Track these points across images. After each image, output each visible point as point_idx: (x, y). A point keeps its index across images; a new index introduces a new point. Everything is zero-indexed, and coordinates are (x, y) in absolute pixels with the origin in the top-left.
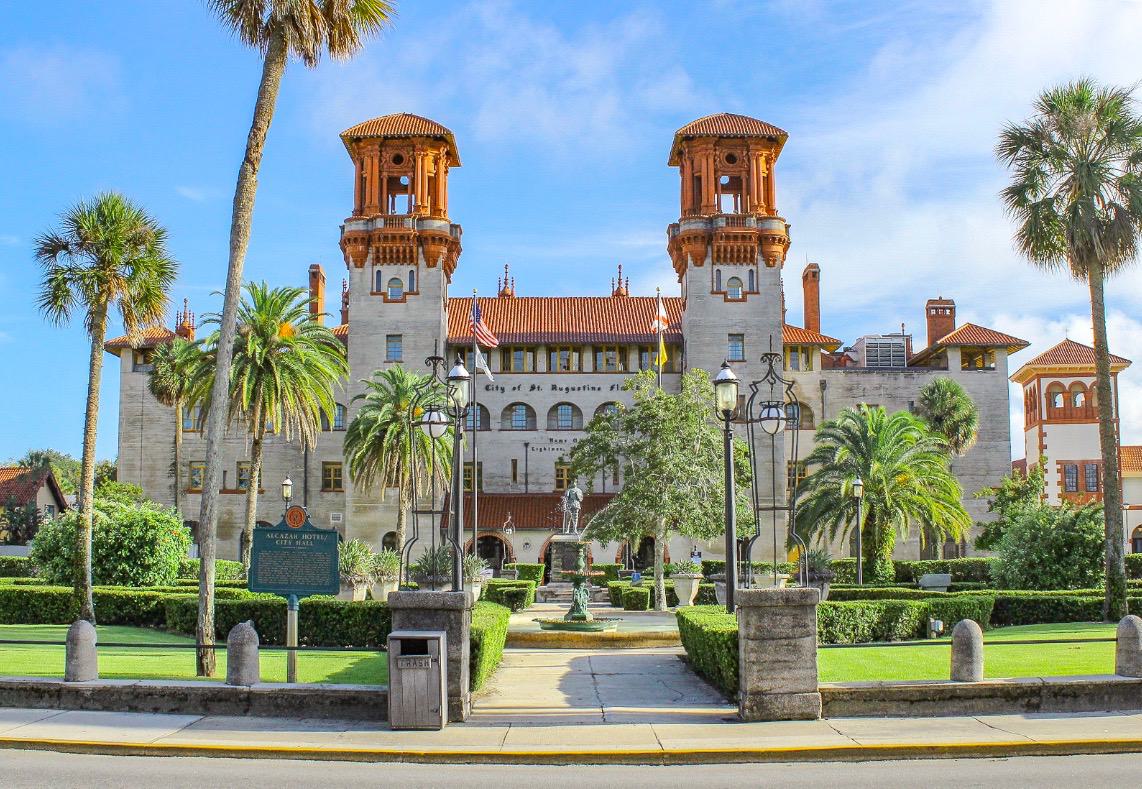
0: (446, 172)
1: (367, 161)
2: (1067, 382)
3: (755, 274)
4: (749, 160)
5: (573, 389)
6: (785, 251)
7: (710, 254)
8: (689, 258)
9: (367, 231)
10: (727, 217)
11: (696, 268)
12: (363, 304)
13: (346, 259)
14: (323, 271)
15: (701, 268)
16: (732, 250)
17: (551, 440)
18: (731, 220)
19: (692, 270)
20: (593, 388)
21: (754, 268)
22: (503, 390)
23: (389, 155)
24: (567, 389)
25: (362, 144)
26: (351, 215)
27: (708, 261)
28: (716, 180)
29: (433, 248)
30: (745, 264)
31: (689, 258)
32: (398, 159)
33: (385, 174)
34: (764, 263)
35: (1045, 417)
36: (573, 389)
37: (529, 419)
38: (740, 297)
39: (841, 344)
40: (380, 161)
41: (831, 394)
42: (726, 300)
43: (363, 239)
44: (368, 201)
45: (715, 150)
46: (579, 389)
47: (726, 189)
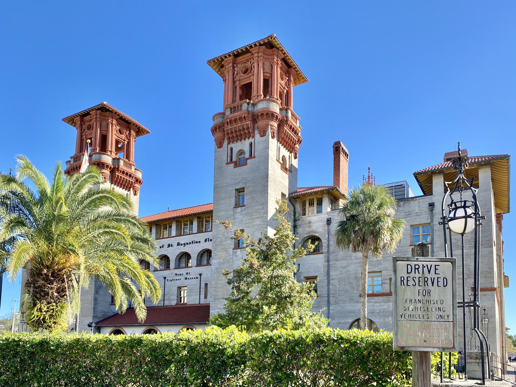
3: (253, 144)
11: (219, 149)
15: (221, 149)
17: (176, 274)
34: (259, 135)
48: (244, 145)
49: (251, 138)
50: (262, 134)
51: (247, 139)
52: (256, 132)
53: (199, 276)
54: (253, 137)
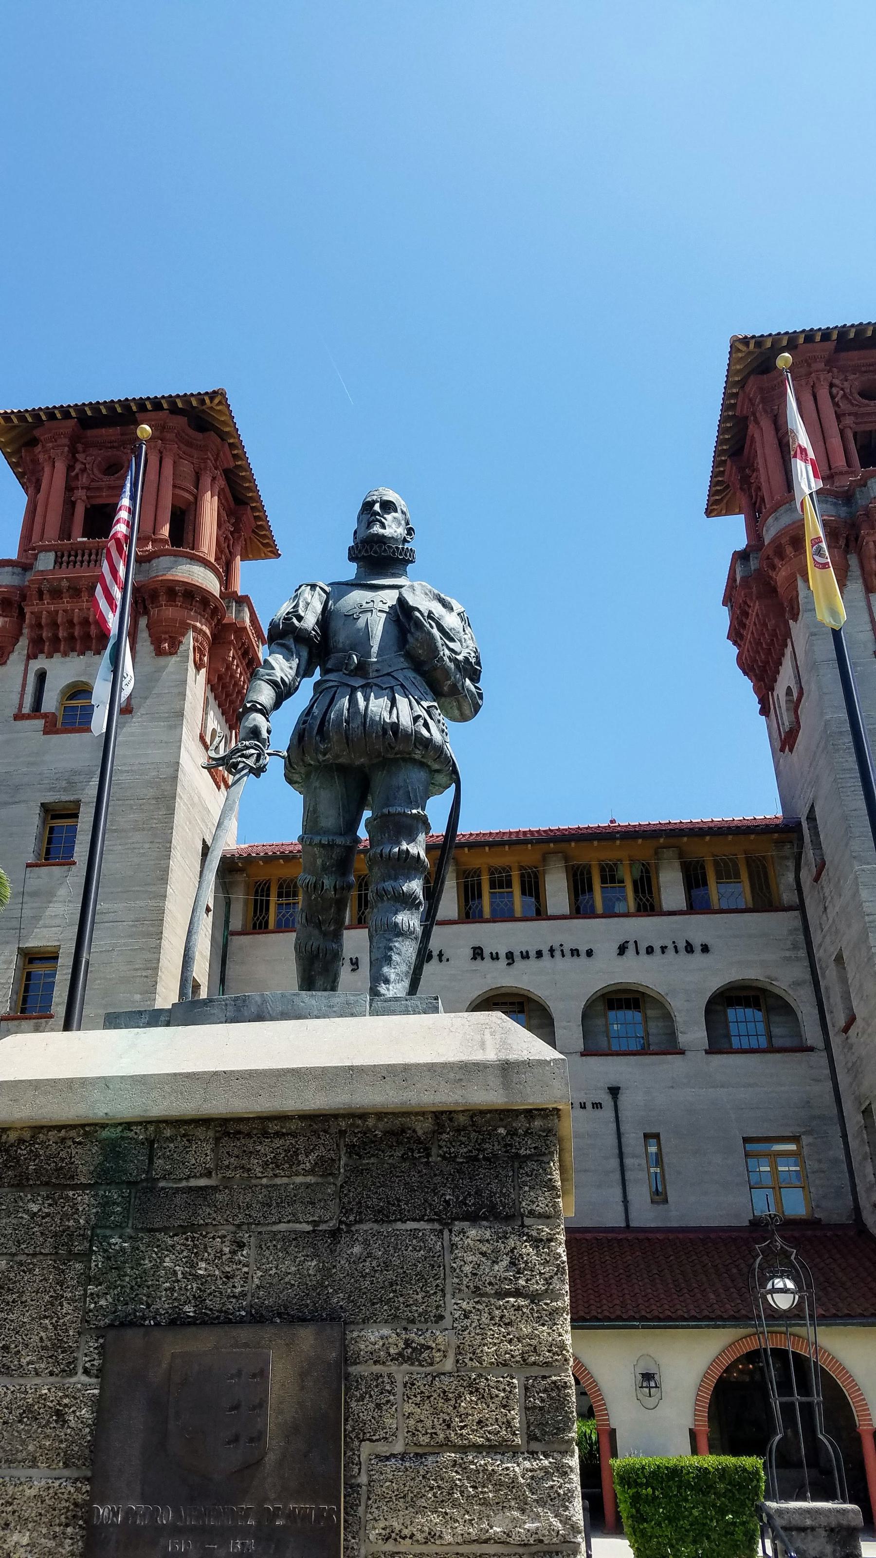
5: (525, 956)
20: (575, 952)
24: (510, 956)
29: (170, 612)
33: (81, 494)
36: (525, 956)
40: (70, 468)
46: (539, 954)
53: (606, 1099)
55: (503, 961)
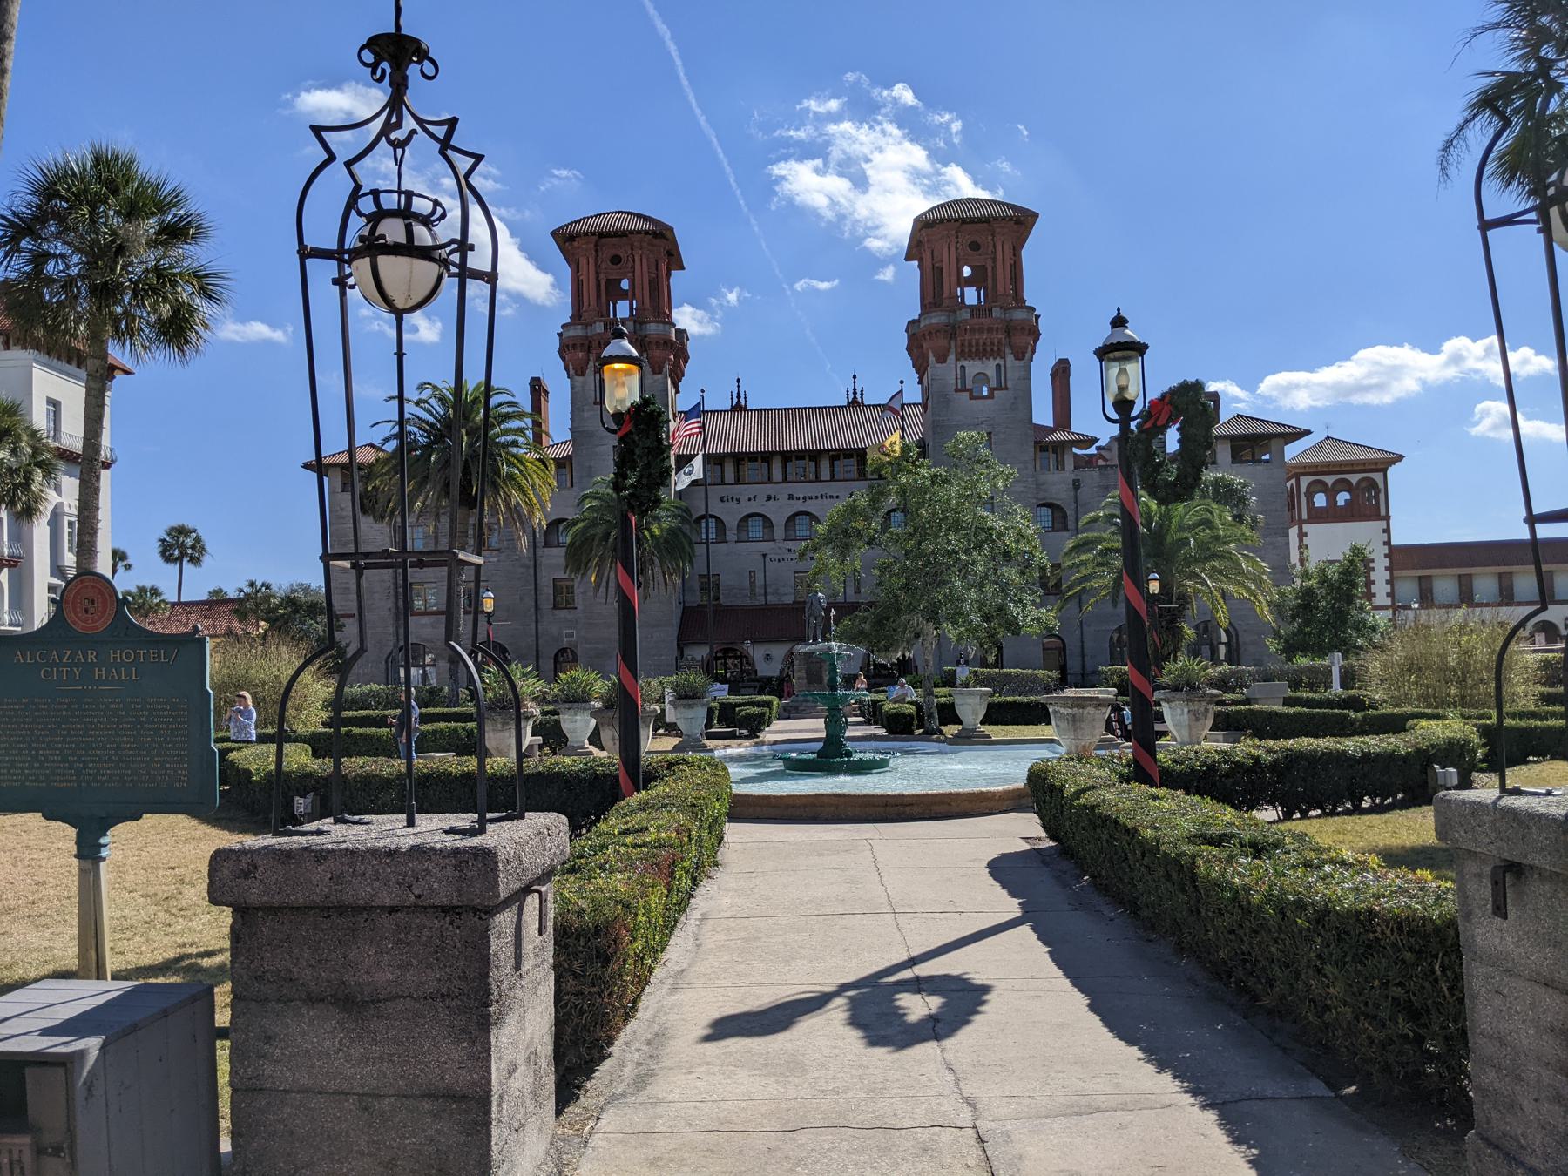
0: (669, 275)
1: (583, 262)
2: (1329, 480)
3: (1003, 368)
4: (994, 246)
5: (811, 498)
6: (1036, 341)
7: (953, 350)
8: (931, 354)
9: (587, 337)
10: (971, 307)
11: (939, 365)
12: (586, 415)
13: (566, 368)
14: (548, 383)
16: (977, 344)
17: (790, 550)
18: (975, 311)
19: (934, 368)
20: (831, 497)
21: (1002, 362)
22: (738, 500)
23: (606, 254)
25: (576, 244)
26: (569, 321)
27: (951, 358)
28: (960, 272)
29: (657, 353)
30: (991, 359)
31: (931, 354)
32: (616, 260)
35: (1305, 516)
36: (811, 498)
37: (766, 530)
38: (985, 393)
39: (1097, 440)
41: (1084, 493)
42: (972, 397)
43: (582, 345)
44: (585, 304)
45: (957, 237)
47: (969, 282)
48: (989, 367)
49: (998, 358)
50: (1020, 356)
51: (991, 359)
52: (1007, 351)
54: (1004, 357)
55: (801, 501)
